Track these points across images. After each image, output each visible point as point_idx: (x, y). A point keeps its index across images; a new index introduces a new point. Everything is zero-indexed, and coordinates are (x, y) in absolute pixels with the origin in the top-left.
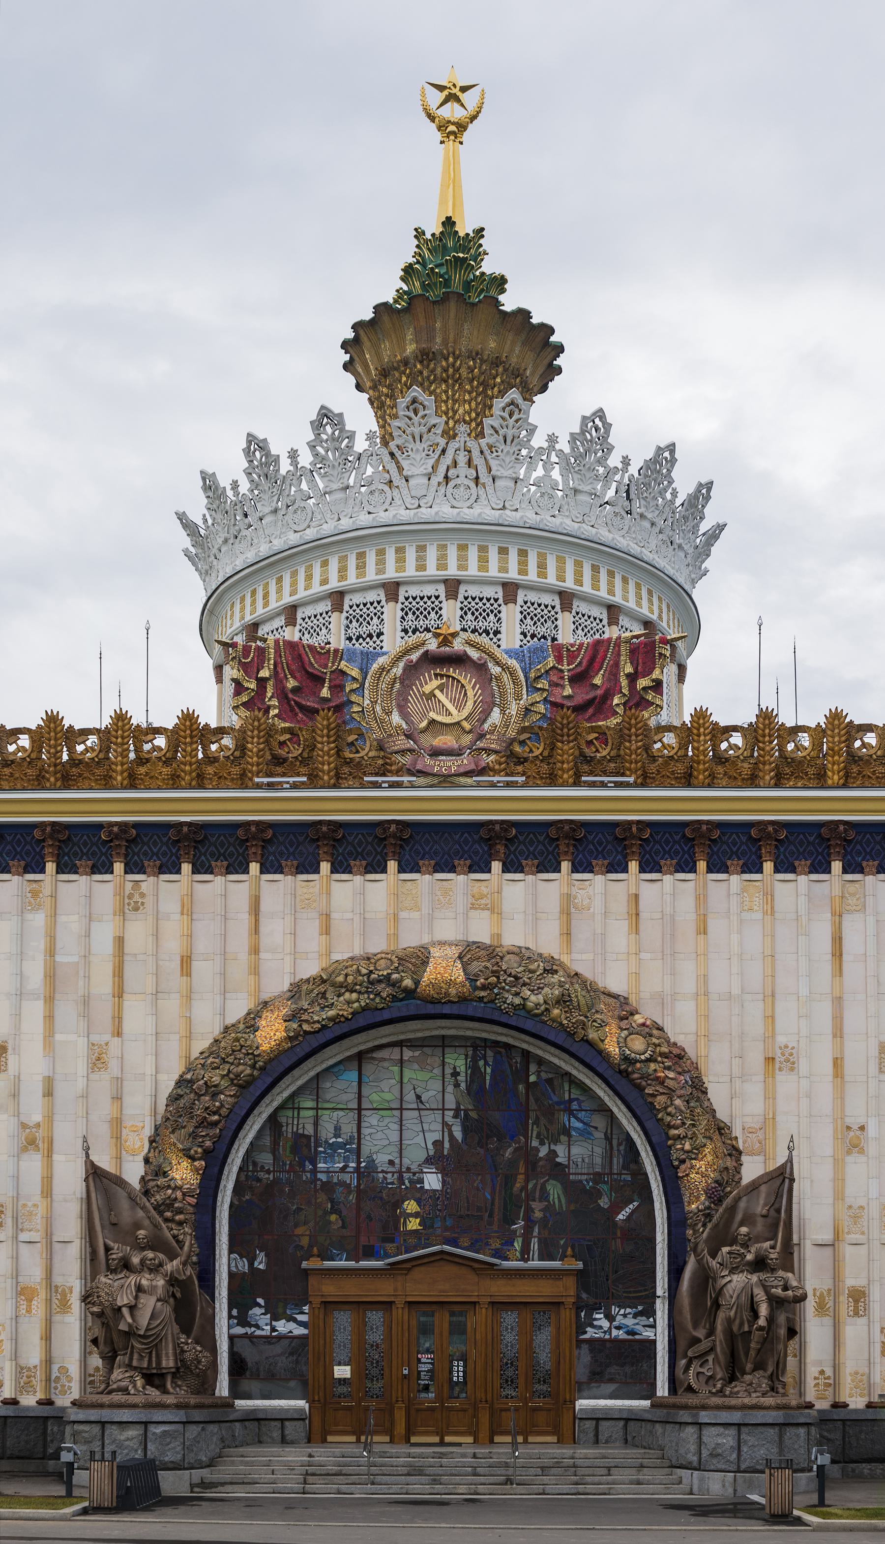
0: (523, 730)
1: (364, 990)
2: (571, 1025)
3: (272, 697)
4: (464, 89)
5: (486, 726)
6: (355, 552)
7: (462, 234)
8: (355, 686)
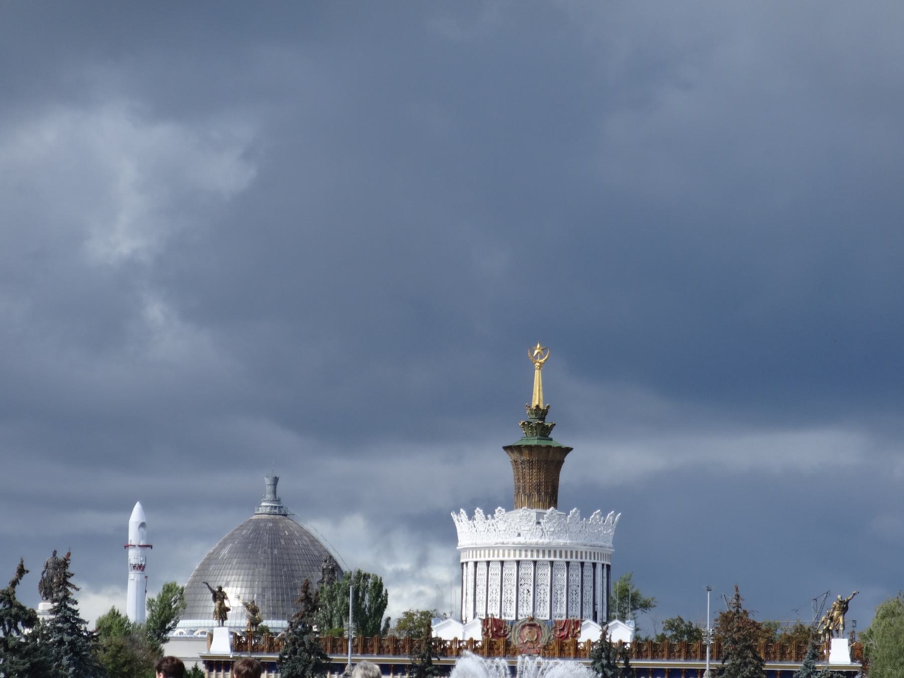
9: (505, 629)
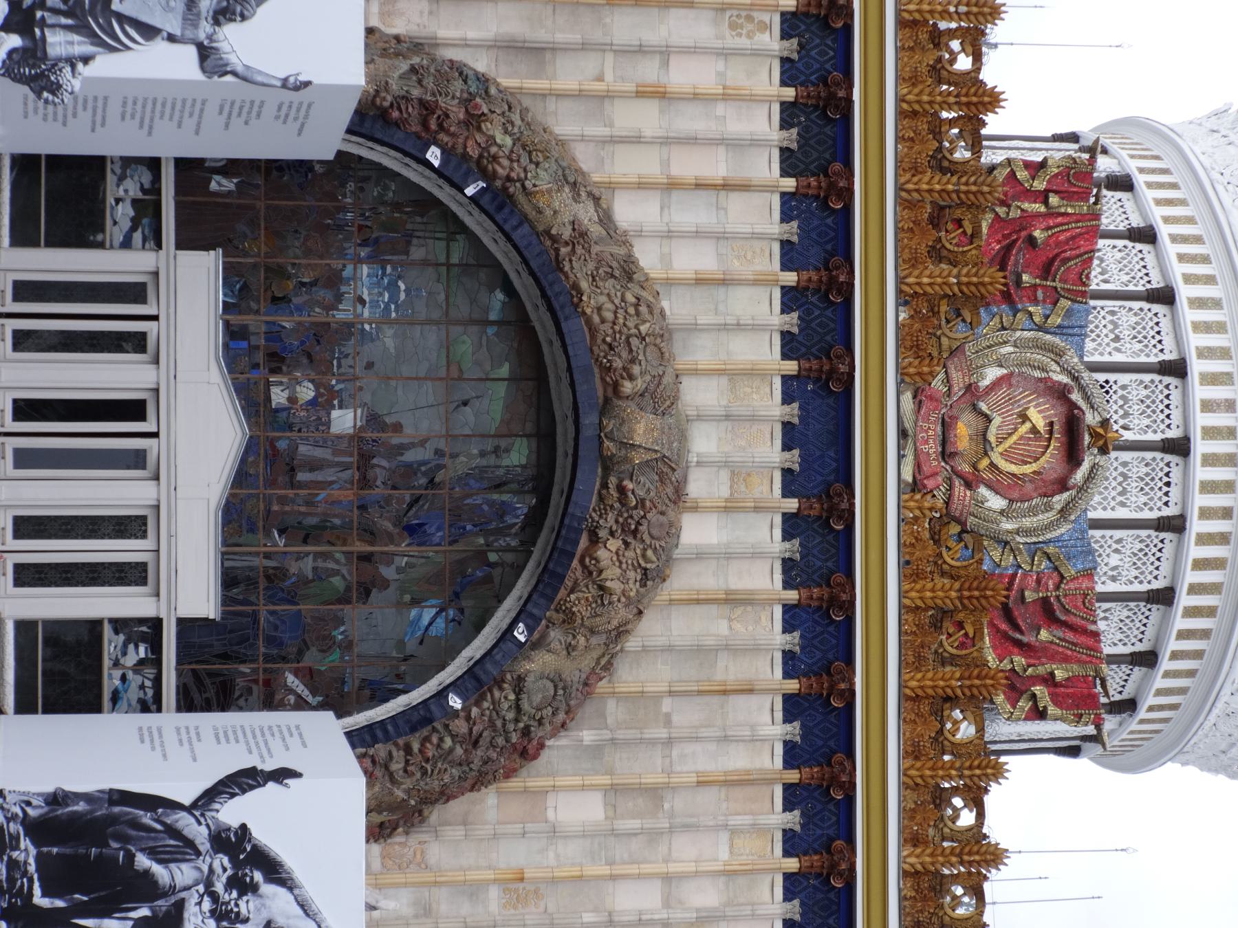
1: (617, 328)
2: (568, 605)
3: (1022, 210)
5: (983, 490)
6: (1227, 319)
8: (1037, 319)
9: (1040, 294)
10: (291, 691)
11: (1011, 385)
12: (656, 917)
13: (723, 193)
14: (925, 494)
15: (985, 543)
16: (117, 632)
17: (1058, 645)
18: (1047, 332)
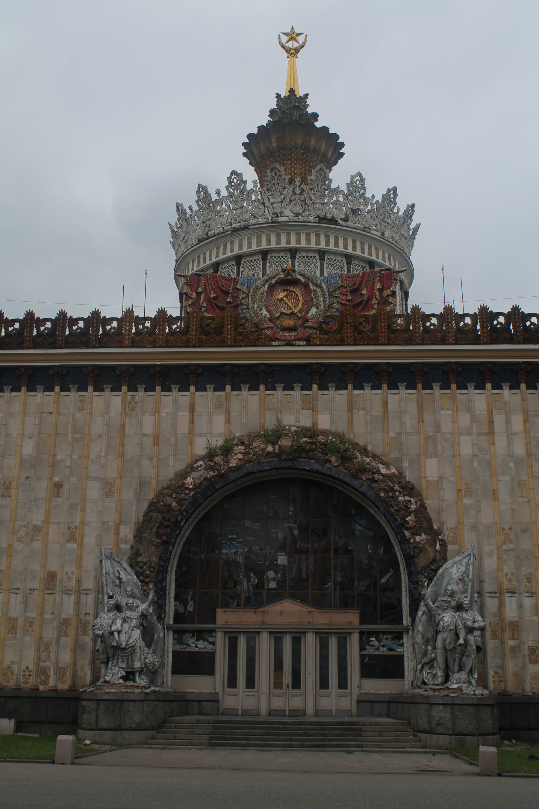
0: (328, 317)
3: (203, 302)
4: (299, 34)
5: (309, 315)
7: (298, 96)
8: (244, 296)
9: (235, 295)
10: (388, 581)
11: (269, 305)
12: (475, 438)
13: (195, 413)
14: (311, 337)
15: (329, 314)
16: (365, 649)
17: (367, 287)
18: (249, 292)
